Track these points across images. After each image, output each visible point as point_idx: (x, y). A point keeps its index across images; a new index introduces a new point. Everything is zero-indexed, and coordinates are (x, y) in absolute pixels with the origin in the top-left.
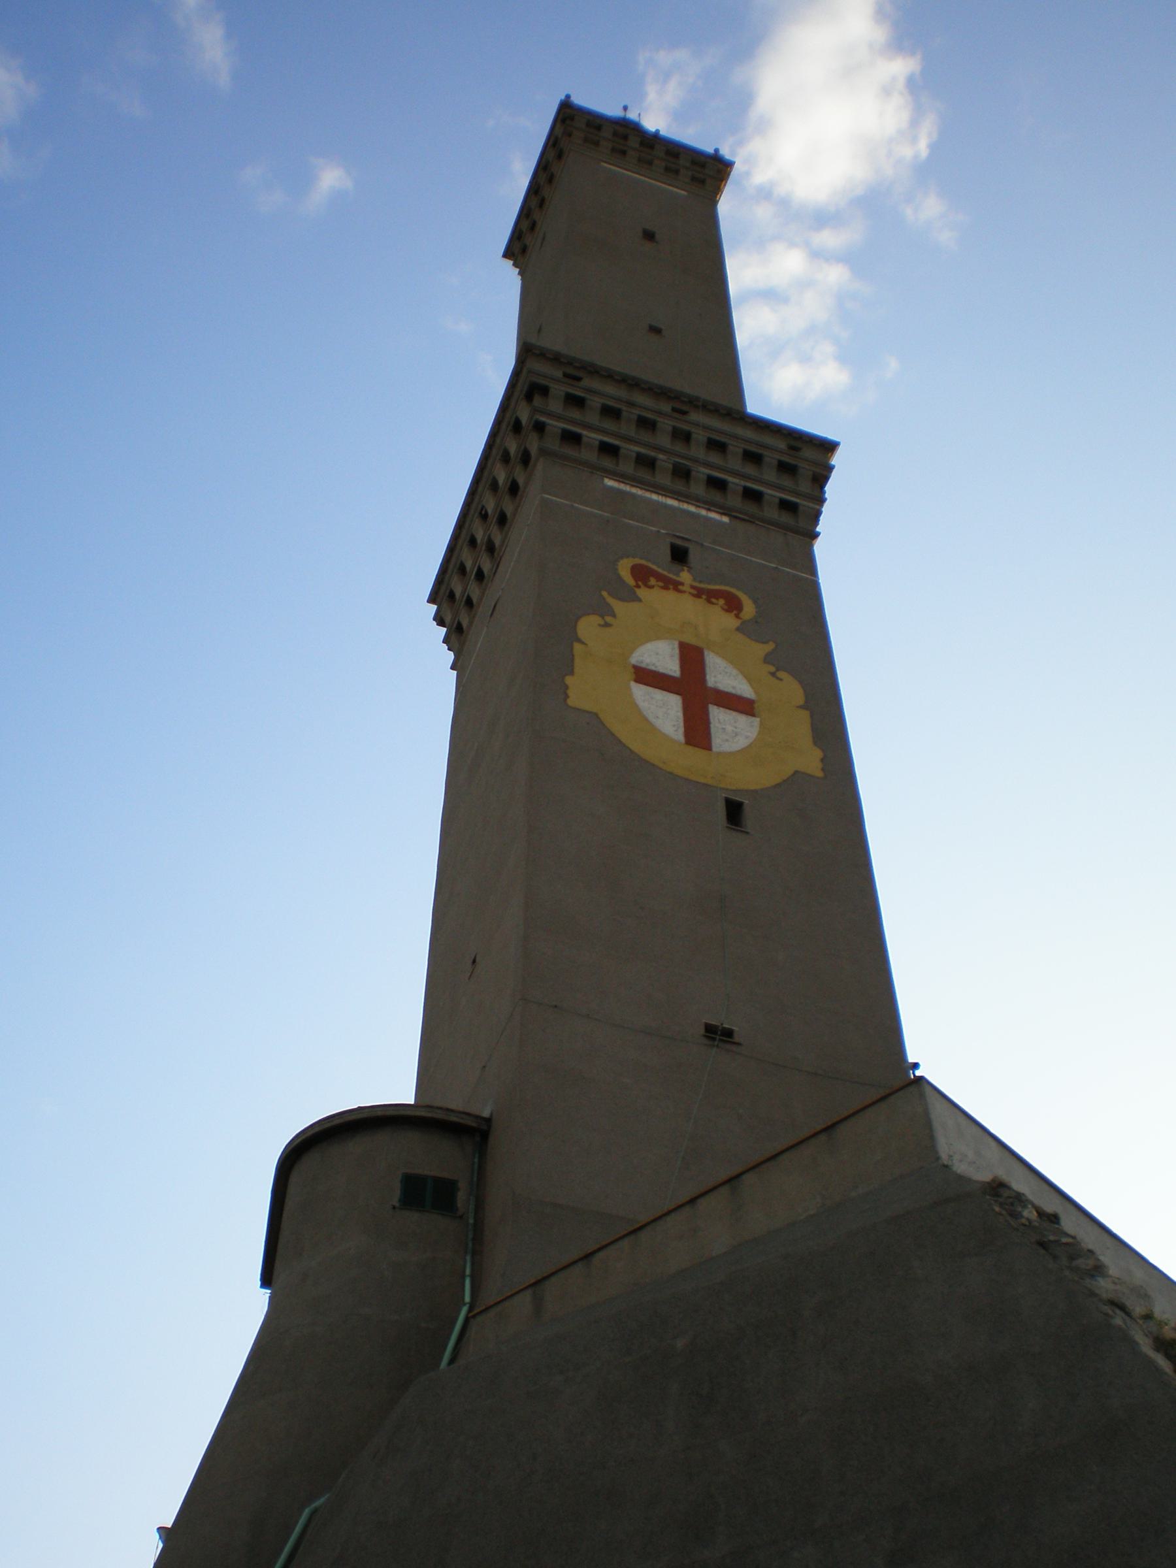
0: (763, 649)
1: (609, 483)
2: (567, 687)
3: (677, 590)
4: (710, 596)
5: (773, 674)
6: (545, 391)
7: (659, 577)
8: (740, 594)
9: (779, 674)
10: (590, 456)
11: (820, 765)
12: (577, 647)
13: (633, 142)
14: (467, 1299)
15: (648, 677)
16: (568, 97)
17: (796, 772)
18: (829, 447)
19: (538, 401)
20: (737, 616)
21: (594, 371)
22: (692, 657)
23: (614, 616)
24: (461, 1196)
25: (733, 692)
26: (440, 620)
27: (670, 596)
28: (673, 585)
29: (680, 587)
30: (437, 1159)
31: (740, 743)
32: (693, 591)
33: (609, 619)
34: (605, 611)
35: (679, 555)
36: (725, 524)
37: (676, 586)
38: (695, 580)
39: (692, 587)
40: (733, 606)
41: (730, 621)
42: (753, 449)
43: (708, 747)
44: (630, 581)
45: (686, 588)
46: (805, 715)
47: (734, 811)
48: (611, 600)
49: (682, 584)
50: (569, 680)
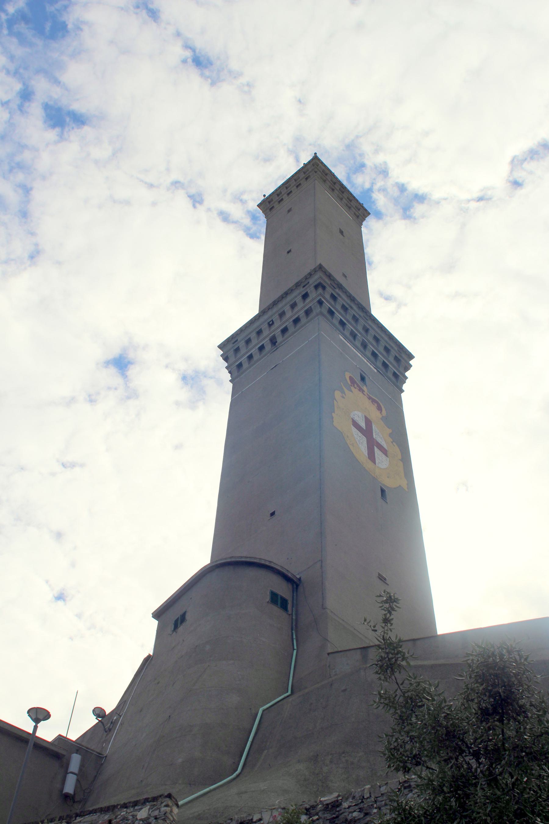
0: (389, 431)
1: (341, 337)
2: (333, 418)
4: (374, 401)
5: (392, 442)
6: (324, 288)
7: (358, 386)
8: (381, 404)
9: (394, 443)
10: (336, 323)
12: (335, 402)
13: (337, 187)
14: (295, 647)
16: (315, 153)
17: (400, 486)
18: (411, 357)
19: (320, 290)
20: (381, 413)
21: (340, 287)
22: (368, 422)
24: (289, 606)
26: (226, 359)
27: (361, 394)
28: (361, 390)
30: (283, 590)
34: (343, 392)
35: (363, 379)
37: (363, 391)
40: (379, 408)
42: (388, 346)
43: (375, 463)
46: (401, 462)
47: (383, 491)
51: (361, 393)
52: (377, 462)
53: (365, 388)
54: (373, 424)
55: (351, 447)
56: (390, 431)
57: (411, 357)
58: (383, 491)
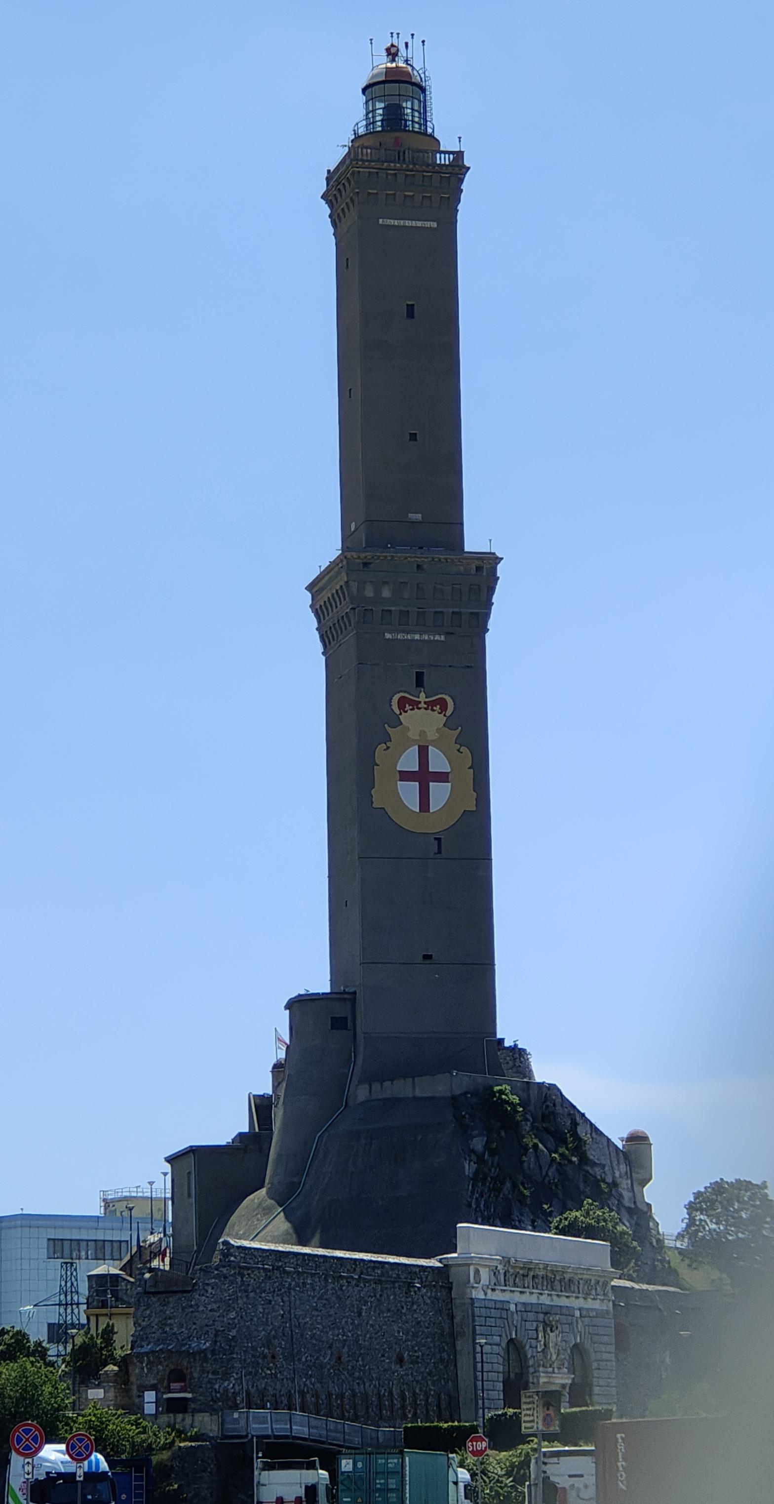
1: (388, 636)
3: (419, 709)
5: (459, 750)
9: (463, 749)
15: (406, 776)
18: (498, 560)
20: (445, 715)
28: (415, 705)
29: (420, 706)
32: (425, 706)
33: (388, 744)
35: (419, 677)
39: (425, 703)
45: (422, 705)
46: (472, 770)
47: (439, 840)
48: (389, 730)
49: (420, 702)
57: (498, 560)
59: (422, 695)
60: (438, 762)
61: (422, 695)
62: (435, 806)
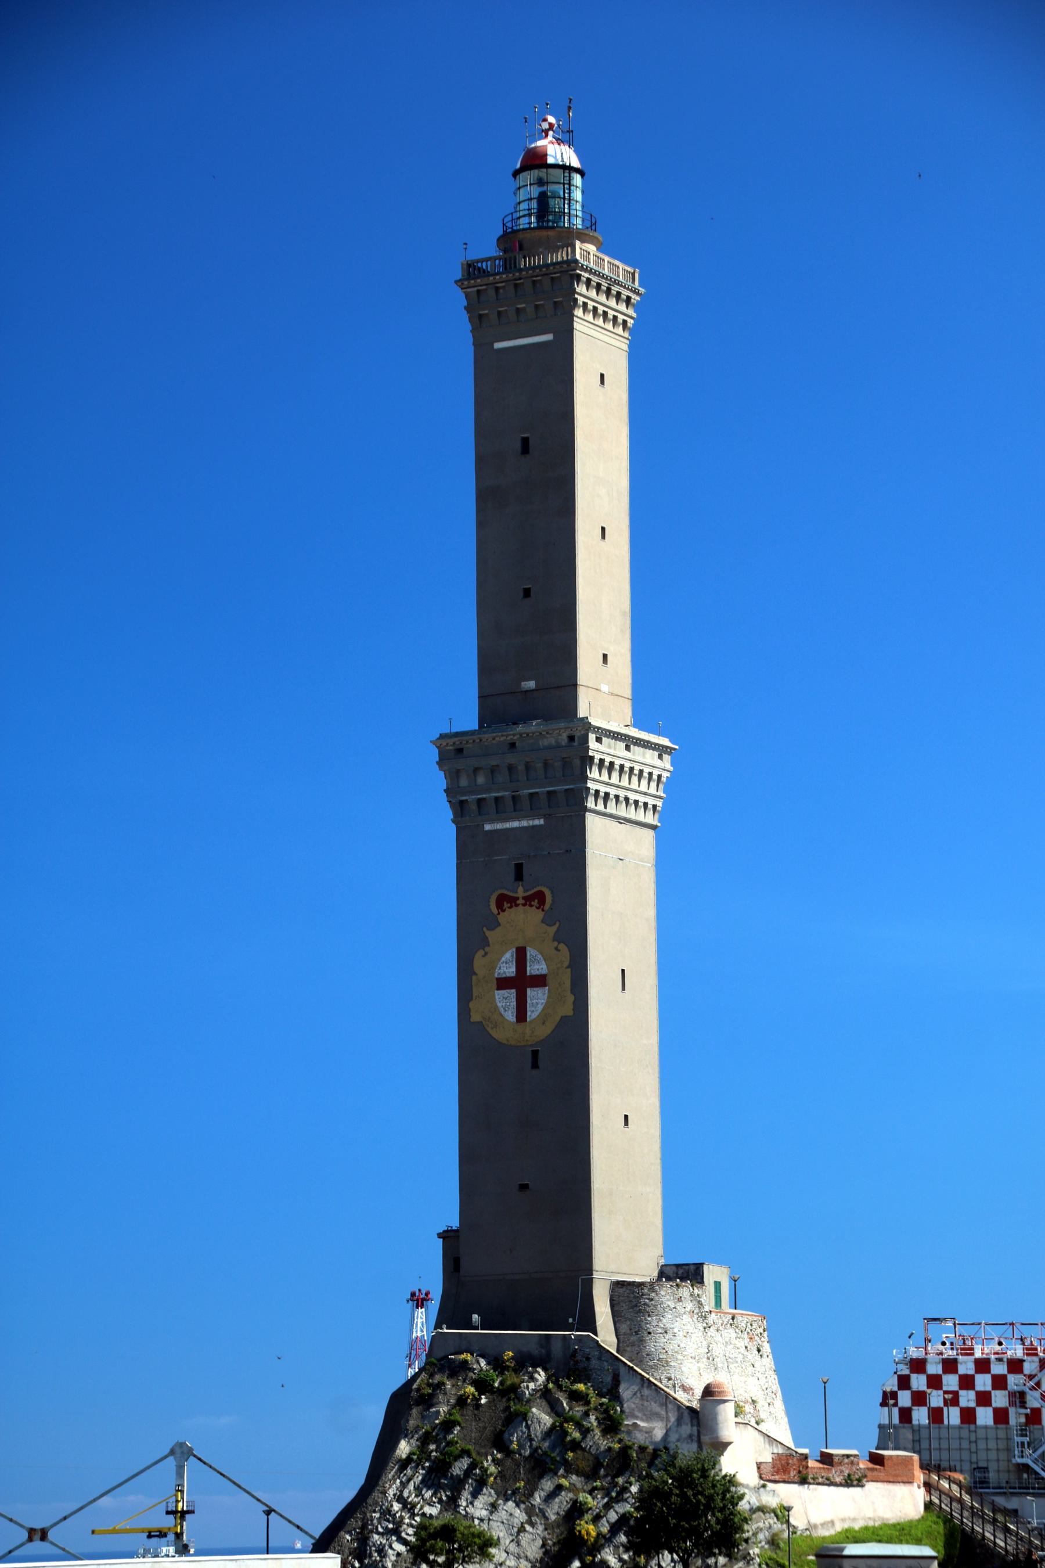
3: (517, 905)
5: (557, 949)
9: (562, 946)
11: (572, 1007)
12: (474, 978)
15: (503, 983)
22: (521, 956)
23: (489, 945)
25: (537, 973)
28: (513, 901)
31: (540, 1008)
33: (487, 949)
34: (485, 943)
35: (519, 873)
36: (541, 826)
38: (526, 891)
39: (524, 898)
41: (540, 915)
44: (495, 911)
45: (521, 901)
46: (569, 970)
47: (535, 1054)
48: (488, 933)
49: (518, 898)
50: (471, 1005)
51: (514, 909)
52: (529, 1014)
53: (521, 893)
54: (528, 949)
55: (493, 1033)
56: (555, 928)
58: (535, 1054)
59: (521, 890)
60: (536, 967)
61: (521, 890)
62: (532, 1014)
